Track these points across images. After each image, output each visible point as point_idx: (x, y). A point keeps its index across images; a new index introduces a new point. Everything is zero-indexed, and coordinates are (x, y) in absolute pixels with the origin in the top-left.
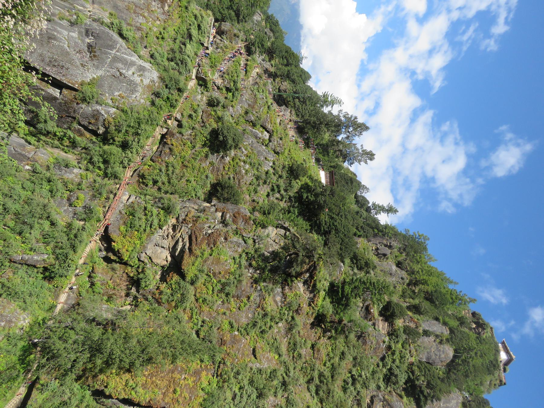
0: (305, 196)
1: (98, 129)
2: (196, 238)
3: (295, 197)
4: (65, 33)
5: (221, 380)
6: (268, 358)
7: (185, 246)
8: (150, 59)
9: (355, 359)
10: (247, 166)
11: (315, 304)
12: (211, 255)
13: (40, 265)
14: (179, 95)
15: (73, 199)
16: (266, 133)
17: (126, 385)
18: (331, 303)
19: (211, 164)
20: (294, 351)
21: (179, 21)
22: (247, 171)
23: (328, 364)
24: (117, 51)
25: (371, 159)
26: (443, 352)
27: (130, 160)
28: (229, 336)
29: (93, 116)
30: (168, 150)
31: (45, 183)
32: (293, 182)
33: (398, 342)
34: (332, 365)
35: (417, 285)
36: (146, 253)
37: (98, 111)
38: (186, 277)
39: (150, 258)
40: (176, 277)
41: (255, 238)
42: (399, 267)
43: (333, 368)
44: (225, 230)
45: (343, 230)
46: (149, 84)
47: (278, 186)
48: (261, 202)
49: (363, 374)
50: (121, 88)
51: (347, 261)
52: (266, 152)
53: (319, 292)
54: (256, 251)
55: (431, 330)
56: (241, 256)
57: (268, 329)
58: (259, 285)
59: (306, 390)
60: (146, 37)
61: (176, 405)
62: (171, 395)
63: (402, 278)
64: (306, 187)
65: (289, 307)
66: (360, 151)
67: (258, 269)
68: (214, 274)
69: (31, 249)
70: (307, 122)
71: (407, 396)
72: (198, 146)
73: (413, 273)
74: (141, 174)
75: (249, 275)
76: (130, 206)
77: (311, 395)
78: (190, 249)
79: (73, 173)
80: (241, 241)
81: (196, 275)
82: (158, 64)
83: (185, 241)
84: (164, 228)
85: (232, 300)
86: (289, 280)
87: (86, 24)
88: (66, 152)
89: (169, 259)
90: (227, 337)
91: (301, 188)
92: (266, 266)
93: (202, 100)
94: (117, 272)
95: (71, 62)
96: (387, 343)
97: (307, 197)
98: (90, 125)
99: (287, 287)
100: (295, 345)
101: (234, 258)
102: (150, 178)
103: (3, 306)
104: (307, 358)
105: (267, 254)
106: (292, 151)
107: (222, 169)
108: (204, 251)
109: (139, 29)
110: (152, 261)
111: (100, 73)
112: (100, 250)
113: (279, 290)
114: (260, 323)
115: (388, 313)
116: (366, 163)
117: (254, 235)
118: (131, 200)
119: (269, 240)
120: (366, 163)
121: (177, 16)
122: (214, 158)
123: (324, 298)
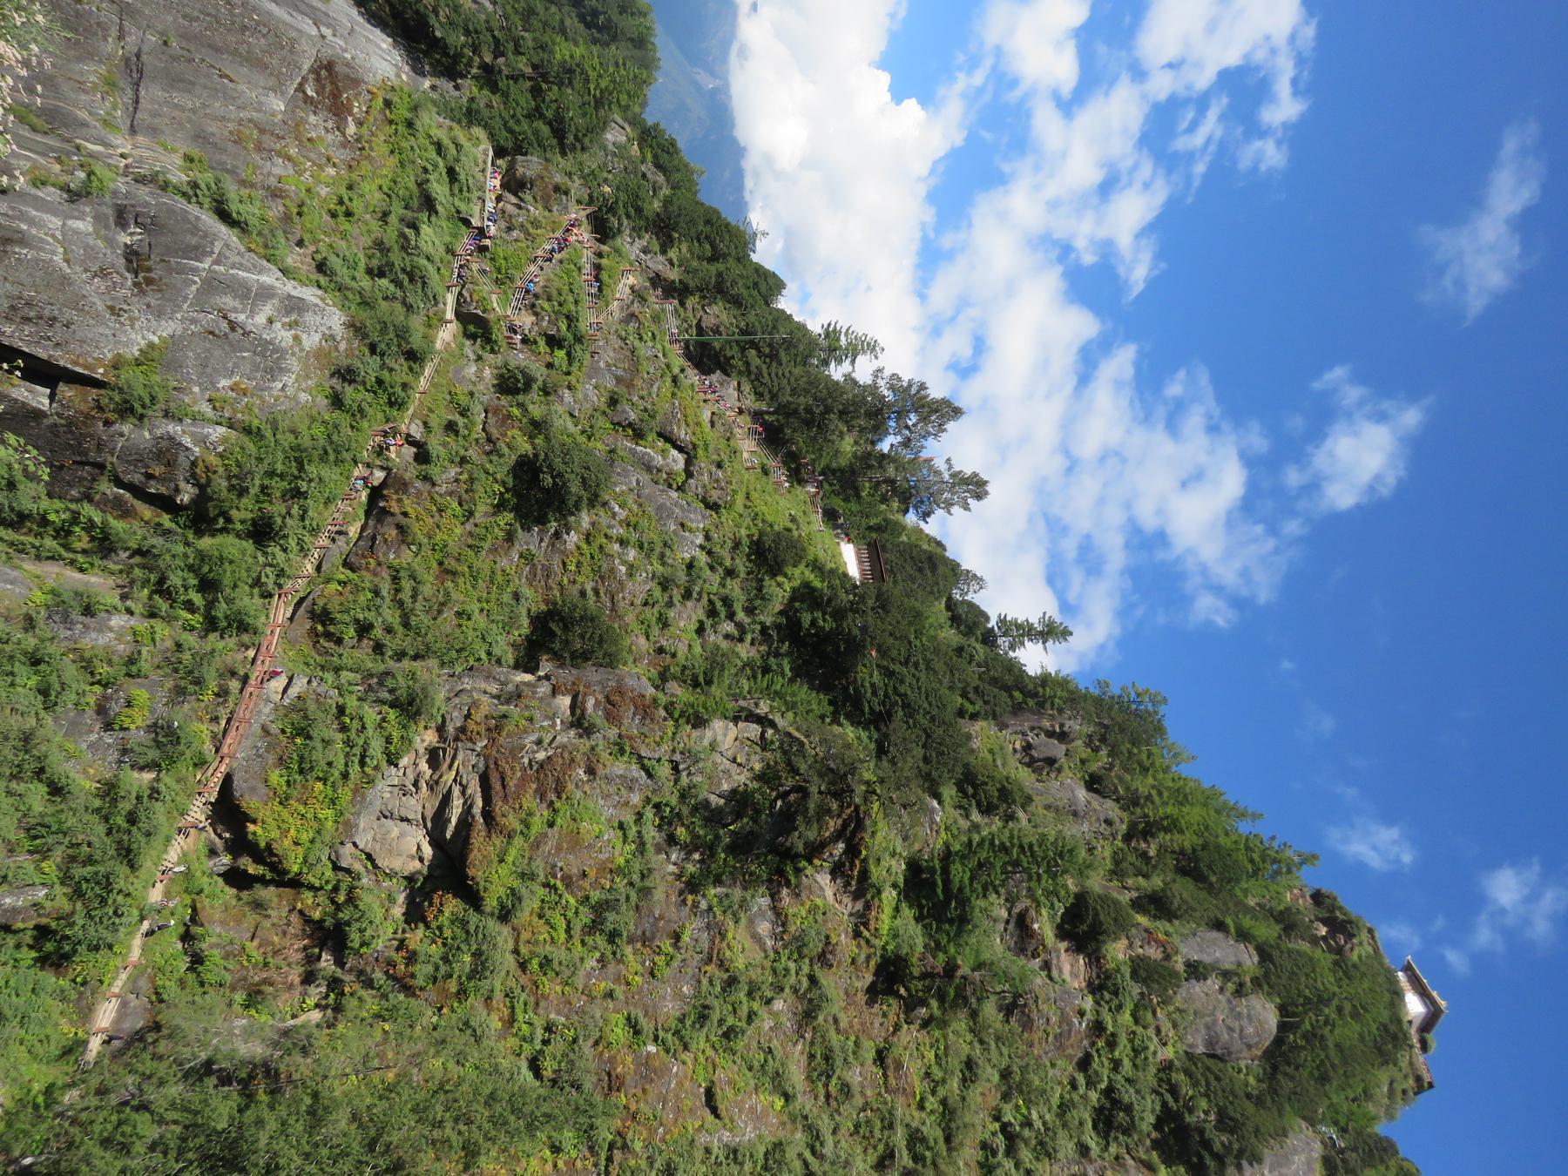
0: (806, 619)
1: (177, 490)
2: (503, 779)
3: (778, 626)
4: (55, 222)
6: (752, 1109)
7: (471, 806)
8: (315, 276)
9: (1005, 1075)
10: (632, 554)
11: (872, 927)
12: (551, 825)
13: (23, 920)
14: (411, 369)
15: (115, 707)
16: (674, 452)
18: (917, 920)
19: (527, 557)
20: (829, 1077)
21: (393, 161)
22: (631, 567)
23: (932, 1103)
24: (217, 262)
25: (979, 497)
26: (1249, 1016)
27: (281, 573)
28: (629, 1059)
30: (394, 532)
31: (22, 670)
32: (767, 582)
33: (1120, 1007)
34: (944, 1102)
35: (1153, 836)
36: (355, 844)
37: (171, 438)
38: (482, 899)
39: (369, 857)
40: (452, 906)
41: (677, 757)
42: (1096, 791)
43: (948, 1113)
44: (584, 744)
45: (926, 705)
46: (321, 348)
47: (727, 601)
48: (682, 651)
49: (1035, 1116)
50: (236, 365)
51: (949, 791)
52: (682, 507)
53: (879, 892)
54: (683, 796)
55: (1207, 959)
56: (640, 815)
57: (743, 1024)
58: (704, 896)
60: (300, 214)
63: (1108, 822)
64: (806, 595)
65: (799, 949)
66: (946, 477)
67: (696, 850)
68: (568, 881)
70: (787, 411)
71: (1168, 1162)
72: (482, 509)
73: (1135, 803)
75: (671, 868)
76: (292, 708)
78: (488, 815)
79: (111, 629)
80: (635, 771)
81: (512, 890)
82: (340, 288)
83: (469, 791)
84: (404, 762)
85: (628, 950)
86: (789, 869)
87: (115, 193)
88: (81, 570)
89: (428, 851)
90: (626, 1066)
91: (793, 599)
92: (717, 837)
93: (481, 378)
94: (270, 912)
95: (79, 303)
96: (1089, 1016)
97: (813, 623)
99: (785, 891)
100: (827, 1058)
101: (621, 826)
102: (347, 618)
104: (869, 1093)
105: (715, 801)
106: (754, 495)
107: (558, 569)
108: (530, 814)
109: (276, 194)
110: (375, 866)
111: (168, 328)
112: (213, 853)
113: (764, 902)
114: (718, 1010)
115: (1083, 929)
116: (966, 507)
117: (674, 751)
118: (294, 691)
119: (718, 759)
120: (966, 507)
121: (385, 149)
122: (531, 541)
123: (897, 909)
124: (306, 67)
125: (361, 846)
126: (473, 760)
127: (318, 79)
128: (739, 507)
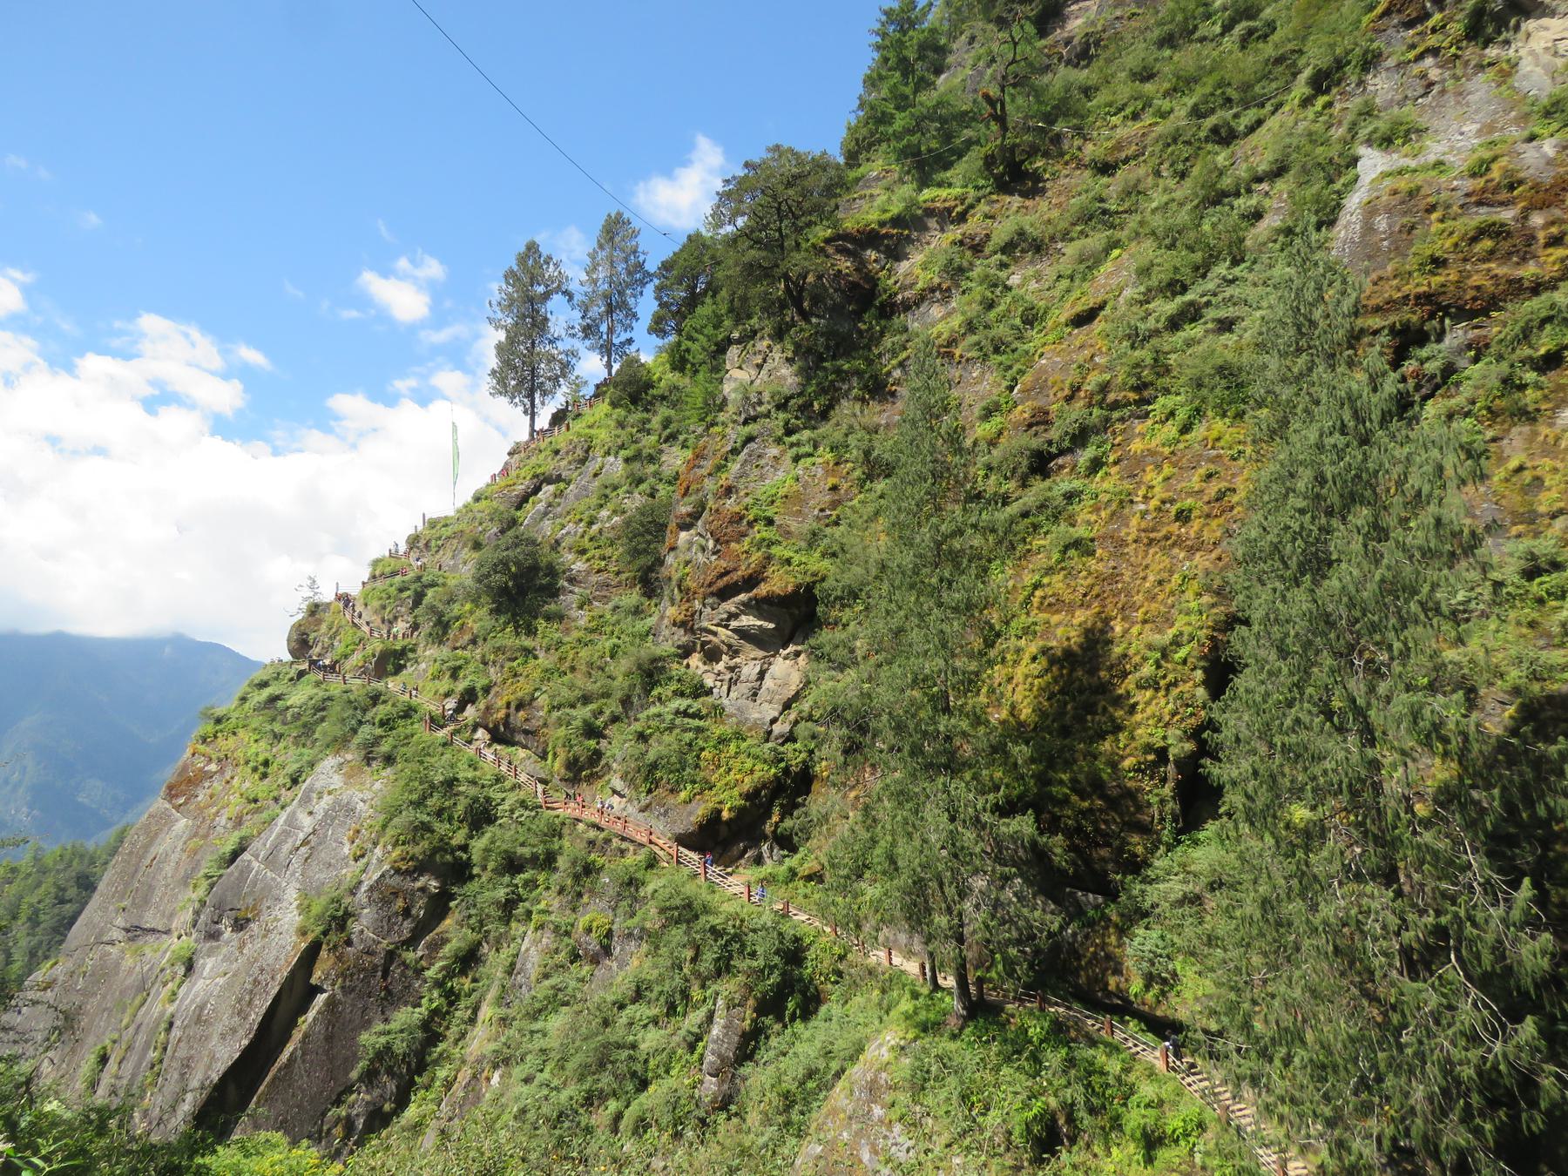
1: (423, 889)
2: (722, 575)
5: (1162, 382)
7: (743, 604)
10: (604, 513)
14: (385, 702)
17: (1152, 684)
20: (1105, 212)
21: (241, 732)
22: (615, 512)
23: (1166, 105)
29: (386, 902)
30: (521, 713)
34: (1167, 94)
36: (774, 721)
37: (371, 889)
39: (787, 706)
44: (711, 504)
54: (782, 406)
56: (792, 445)
59: (1254, 139)
60: (256, 801)
61: (1235, 499)
62: (1196, 524)
68: (835, 504)
69: (692, 1048)
72: (528, 642)
77: (1273, 113)
79: (527, 950)
82: (312, 765)
84: (709, 681)
87: (196, 941)
89: (791, 648)
90: (1023, 412)
95: (251, 962)
98: (414, 912)
100: (1090, 219)
101: (796, 459)
103: (826, 1117)
107: (602, 577)
110: (796, 697)
111: (292, 894)
112: (759, 861)
116: (635, 234)
117: (734, 422)
118: (617, 783)
121: (232, 739)
122: (569, 600)
123: (940, 185)
124: (168, 806)
125: (776, 714)
126: (709, 609)
127: (176, 796)
128: (593, 432)
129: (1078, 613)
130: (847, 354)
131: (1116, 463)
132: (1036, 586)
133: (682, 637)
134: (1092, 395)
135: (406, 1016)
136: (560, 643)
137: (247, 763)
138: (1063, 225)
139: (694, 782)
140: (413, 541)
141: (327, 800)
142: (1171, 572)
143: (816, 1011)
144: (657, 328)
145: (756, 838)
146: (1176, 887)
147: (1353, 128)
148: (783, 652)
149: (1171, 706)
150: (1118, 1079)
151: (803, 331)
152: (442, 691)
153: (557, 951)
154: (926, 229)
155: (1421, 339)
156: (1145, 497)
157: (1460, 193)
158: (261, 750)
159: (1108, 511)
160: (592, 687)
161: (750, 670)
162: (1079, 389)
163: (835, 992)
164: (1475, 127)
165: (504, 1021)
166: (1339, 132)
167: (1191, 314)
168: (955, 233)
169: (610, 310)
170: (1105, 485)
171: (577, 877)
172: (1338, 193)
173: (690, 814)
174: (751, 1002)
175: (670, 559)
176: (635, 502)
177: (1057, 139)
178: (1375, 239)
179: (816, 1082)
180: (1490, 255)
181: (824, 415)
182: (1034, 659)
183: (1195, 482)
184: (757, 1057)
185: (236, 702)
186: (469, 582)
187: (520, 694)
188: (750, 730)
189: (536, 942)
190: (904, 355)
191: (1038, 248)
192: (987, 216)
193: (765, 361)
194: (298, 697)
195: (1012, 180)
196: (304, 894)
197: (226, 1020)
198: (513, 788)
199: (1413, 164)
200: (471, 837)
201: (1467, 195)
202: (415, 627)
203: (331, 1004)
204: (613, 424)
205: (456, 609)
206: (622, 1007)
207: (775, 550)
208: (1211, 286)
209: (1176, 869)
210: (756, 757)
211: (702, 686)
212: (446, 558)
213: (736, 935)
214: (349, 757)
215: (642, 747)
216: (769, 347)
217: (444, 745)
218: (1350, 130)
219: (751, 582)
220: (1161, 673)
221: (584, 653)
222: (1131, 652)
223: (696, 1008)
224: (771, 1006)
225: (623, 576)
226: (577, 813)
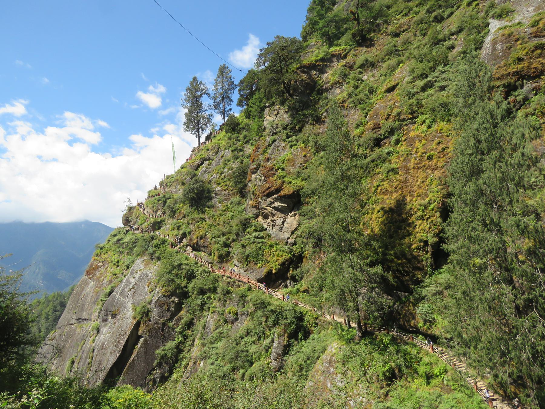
1: (173, 301)
2: (267, 189)
7: (275, 198)
10: (226, 170)
11: (341, 52)
12: (283, 169)
20: (397, 50)
21: (109, 252)
22: (229, 169)
23: (417, 9)
31: (214, 345)
34: (417, 6)
36: (288, 238)
37: (156, 302)
39: (293, 233)
44: (262, 164)
54: (285, 129)
56: (289, 142)
58: (322, 114)
59: (450, 19)
60: (116, 275)
61: (449, 151)
62: (435, 161)
68: (305, 162)
69: (267, 351)
72: (202, 216)
74: (220, 260)
76: (241, 262)
77: (457, 9)
80: (272, 147)
82: (133, 262)
84: (265, 226)
87: (100, 322)
89: (293, 213)
90: (370, 125)
98: (171, 309)
100: (391, 54)
101: (291, 147)
103: (315, 372)
106: (219, 138)
110: (296, 230)
111: (130, 305)
112: (286, 286)
116: (230, 71)
117: (269, 135)
118: (236, 262)
119: (276, 120)
121: (106, 254)
122: (215, 201)
123: (337, 45)
126: (263, 201)
127: (90, 274)
128: (220, 142)
129: (393, 195)
130: (307, 109)
131: (405, 141)
132: (378, 186)
133: (255, 211)
134: (395, 117)
135: (170, 344)
136: (213, 216)
137: (112, 262)
138: (382, 56)
139: (262, 261)
140: (161, 184)
141: (139, 273)
142: (426, 178)
143: (308, 337)
144: (240, 104)
145: (285, 279)
146: (433, 289)
147: (487, 12)
148: (290, 214)
149: (428, 226)
150: (416, 356)
151: (291, 101)
152: (175, 234)
153: (219, 320)
154: (332, 62)
155: (515, 88)
156: (416, 152)
157: (528, 33)
158: (116, 257)
159: (403, 158)
160: (225, 230)
161: (279, 221)
162: (390, 115)
163: (315, 330)
164: (531, 9)
165: (203, 345)
166: (482, 14)
167: (430, 85)
168: (343, 62)
169: (223, 99)
170: (401, 149)
171: (224, 295)
172: (482, 37)
173: (262, 272)
174: (286, 335)
175: (249, 184)
176: (236, 165)
177: (378, 25)
178: (497, 53)
179: (310, 361)
180: (540, 55)
181: (300, 130)
182: (379, 212)
183: (434, 145)
184: (289, 353)
185: (107, 242)
186: (181, 197)
187: (201, 234)
188: (280, 242)
189: (212, 318)
190: (327, 107)
191: (373, 65)
192: (354, 55)
193: (278, 113)
194: (127, 239)
195: (362, 42)
196: (134, 305)
197: (111, 348)
198: (201, 266)
199: (510, 24)
200: (188, 283)
201: (531, 34)
202: (164, 213)
203: (145, 341)
204: (227, 139)
205: (177, 206)
206: (242, 338)
207: (285, 179)
208: (436, 74)
209: (433, 283)
210: (283, 251)
211: (263, 228)
212: (173, 189)
213: (280, 312)
214: (145, 258)
215: (244, 249)
216: (279, 108)
217: (177, 252)
218: (486, 13)
219: (278, 190)
220: (424, 214)
221: (222, 219)
222: (413, 207)
223: (268, 337)
224: (293, 336)
225: (234, 191)
226: (223, 273)
